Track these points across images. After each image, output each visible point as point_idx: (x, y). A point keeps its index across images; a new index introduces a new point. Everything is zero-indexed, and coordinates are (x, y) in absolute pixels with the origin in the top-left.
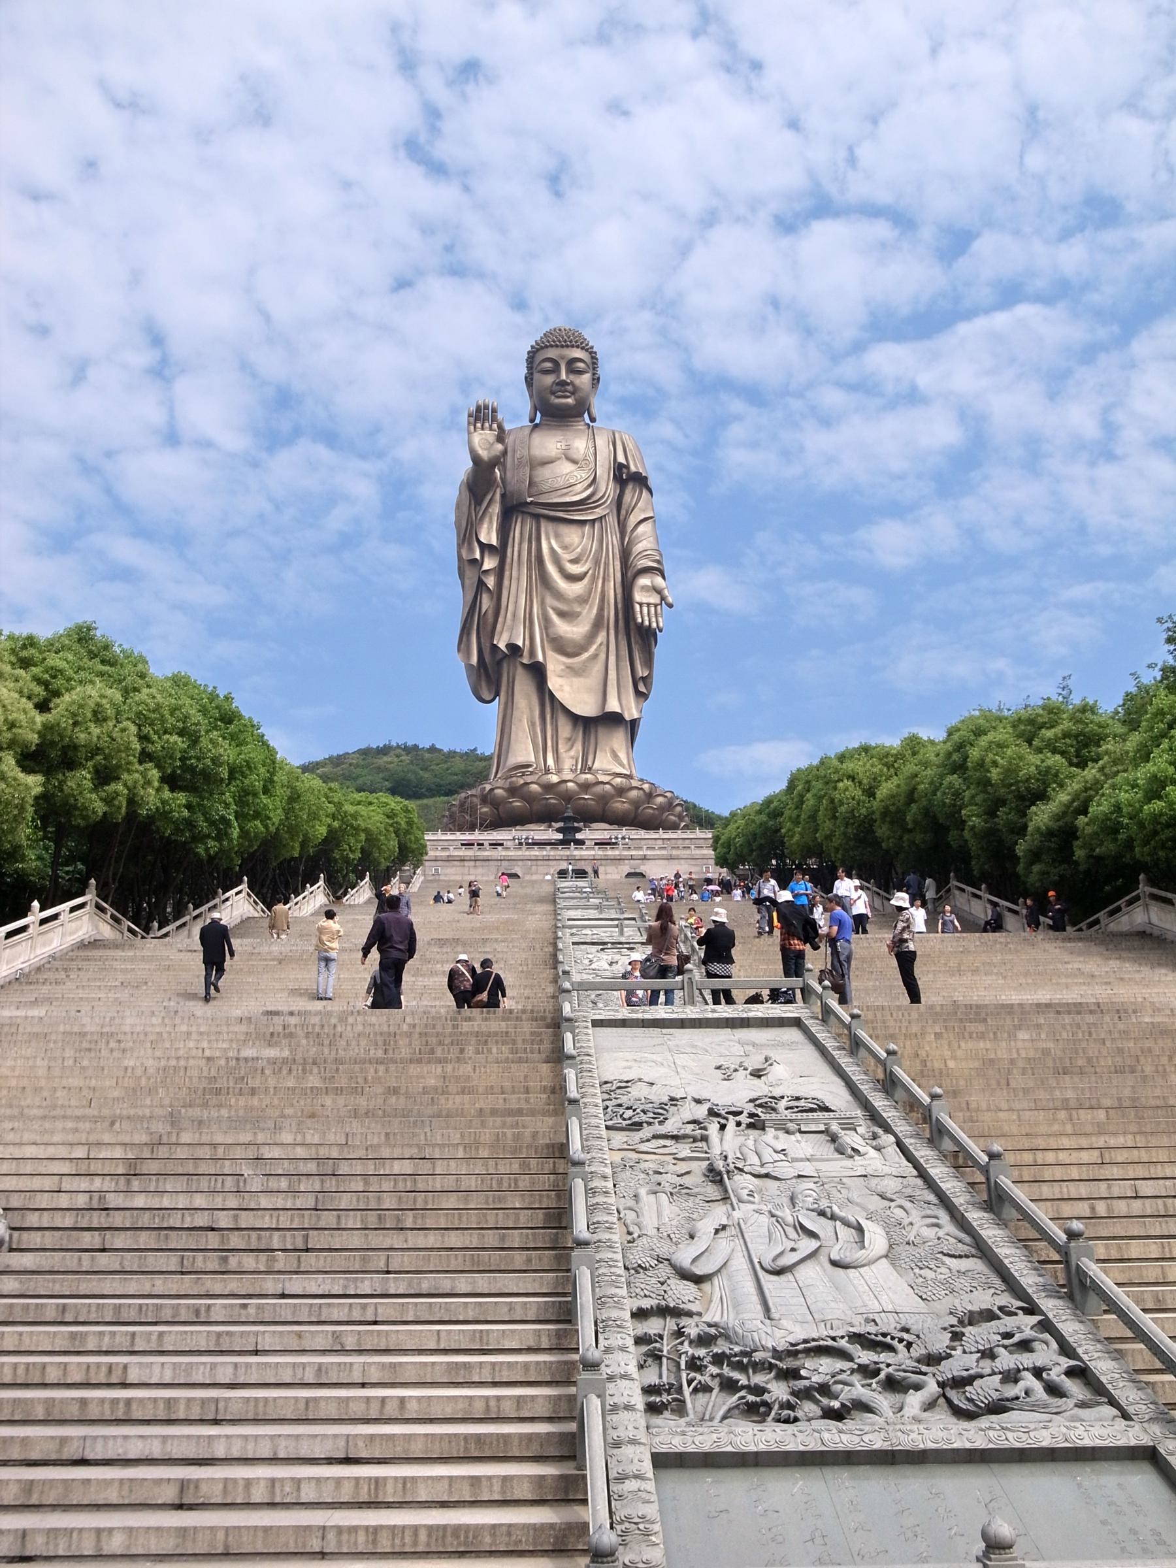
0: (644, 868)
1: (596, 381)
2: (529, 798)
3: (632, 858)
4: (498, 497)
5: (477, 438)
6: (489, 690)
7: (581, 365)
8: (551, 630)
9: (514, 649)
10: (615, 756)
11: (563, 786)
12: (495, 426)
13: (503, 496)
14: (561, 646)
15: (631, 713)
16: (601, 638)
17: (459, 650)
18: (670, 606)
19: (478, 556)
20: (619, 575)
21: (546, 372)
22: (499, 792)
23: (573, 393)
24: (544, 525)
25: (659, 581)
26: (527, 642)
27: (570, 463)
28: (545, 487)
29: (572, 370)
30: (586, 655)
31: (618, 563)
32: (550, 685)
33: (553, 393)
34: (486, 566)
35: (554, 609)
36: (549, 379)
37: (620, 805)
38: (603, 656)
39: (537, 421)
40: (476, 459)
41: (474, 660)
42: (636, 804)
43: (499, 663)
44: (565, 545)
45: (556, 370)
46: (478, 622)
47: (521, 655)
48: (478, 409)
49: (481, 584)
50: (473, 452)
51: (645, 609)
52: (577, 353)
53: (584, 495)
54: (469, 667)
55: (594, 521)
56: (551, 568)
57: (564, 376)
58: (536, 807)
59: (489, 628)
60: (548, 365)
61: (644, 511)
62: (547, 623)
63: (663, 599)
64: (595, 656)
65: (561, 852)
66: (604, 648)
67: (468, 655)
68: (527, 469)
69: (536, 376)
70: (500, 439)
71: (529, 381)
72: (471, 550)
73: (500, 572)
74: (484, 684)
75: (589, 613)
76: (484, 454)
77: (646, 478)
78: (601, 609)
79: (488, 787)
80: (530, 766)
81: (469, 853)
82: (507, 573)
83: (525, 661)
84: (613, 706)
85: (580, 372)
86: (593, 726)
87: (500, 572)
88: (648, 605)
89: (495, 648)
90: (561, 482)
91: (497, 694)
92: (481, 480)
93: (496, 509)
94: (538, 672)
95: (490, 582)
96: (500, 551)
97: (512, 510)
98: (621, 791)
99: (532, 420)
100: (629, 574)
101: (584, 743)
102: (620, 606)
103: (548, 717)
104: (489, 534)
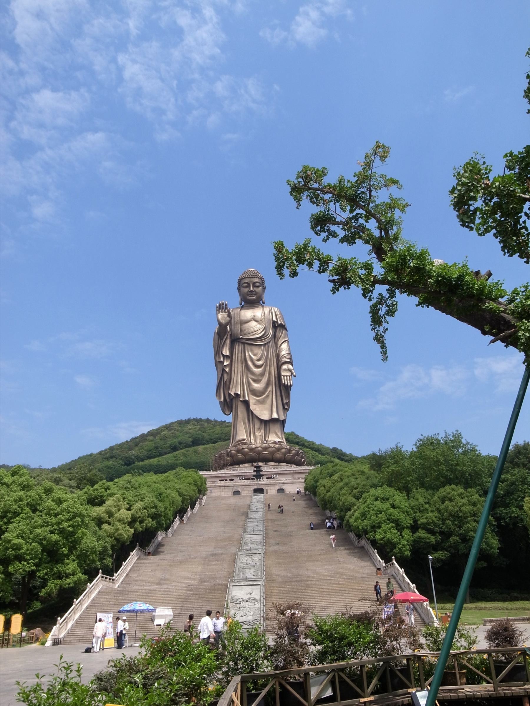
0: (284, 487)
1: (264, 289)
2: (244, 454)
3: (279, 483)
4: (229, 336)
5: (220, 317)
6: (229, 411)
7: (258, 284)
8: (250, 387)
9: (237, 394)
10: (277, 434)
11: (257, 449)
12: (227, 311)
13: (231, 335)
14: (254, 393)
15: (282, 418)
16: (270, 389)
17: (216, 395)
18: (295, 376)
19: (222, 360)
20: (275, 364)
21: (245, 287)
22: (233, 452)
23: (256, 295)
24: (246, 346)
25: (290, 367)
26: (242, 392)
27: (255, 320)
28: (246, 332)
29: (254, 286)
30: (264, 396)
31: (275, 359)
32: (251, 408)
33: (248, 295)
34: (225, 364)
35: (252, 379)
36: (246, 290)
37: (278, 455)
38: (271, 396)
39: (243, 304)
40: (220, 324)
41: (222, 399)
42: (285, 454)
43: (231, 400)
44: (253, 354)
45: (249, 286)
46: (223, 384)
47: (240, 397)
48: (220, 305)
49: (224, 370)
50: (218, 321)
51: (285, 378)
52: (256, 280)
53: (261, 335)
54: (220, 402)
55: (265, 344)
56: (250, 363)
57: (252, 289)
58: (247, 457)
59: (228, 386)
60: (246, 285)
61: (284, 338)
62: (249, 384)
63: (292, 373)
64: (268, 396)
65: (255, 482)
66: (271, 393)
67: (220, 398)
68: (240, 325)
69: (242, 289)
70: (229, 315)
71: (239, 290)
72: (220, 358)
73: (230, 365)
74: (226, 408)
75: (265, 380)
76: (223, 322)
77: (284, 326)
78: (269, 378)
79: (229, 450)
80: (244, 440)
81: (223, 483)
82: (233, 365)
83: (241, 399)
84: (275, 416)
85: (258, 287)
86: (266, 424)
87: (230, 365)
88: (287, 376)
89: (230, 394)
90: (252, 330)
91: (231, 411)
92: (222, 332)
93: (228, 341)
94: (246, 403)
95: (227, 370)
96: (230, 357)
97: (235, 341)
98: (279, 450)
99: (241, 305)
100: (280, 364)
101: (265, 431)
102: (276, 376)
103: (251, 420)
104: (226, 352)
